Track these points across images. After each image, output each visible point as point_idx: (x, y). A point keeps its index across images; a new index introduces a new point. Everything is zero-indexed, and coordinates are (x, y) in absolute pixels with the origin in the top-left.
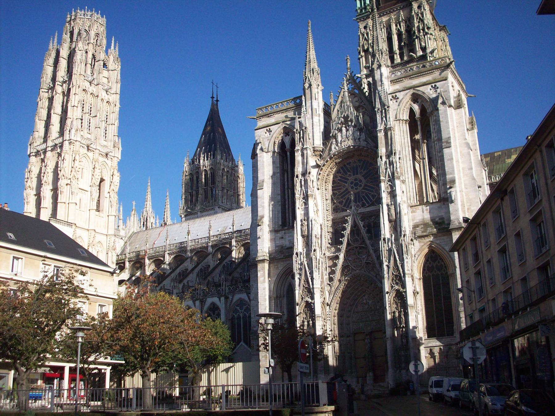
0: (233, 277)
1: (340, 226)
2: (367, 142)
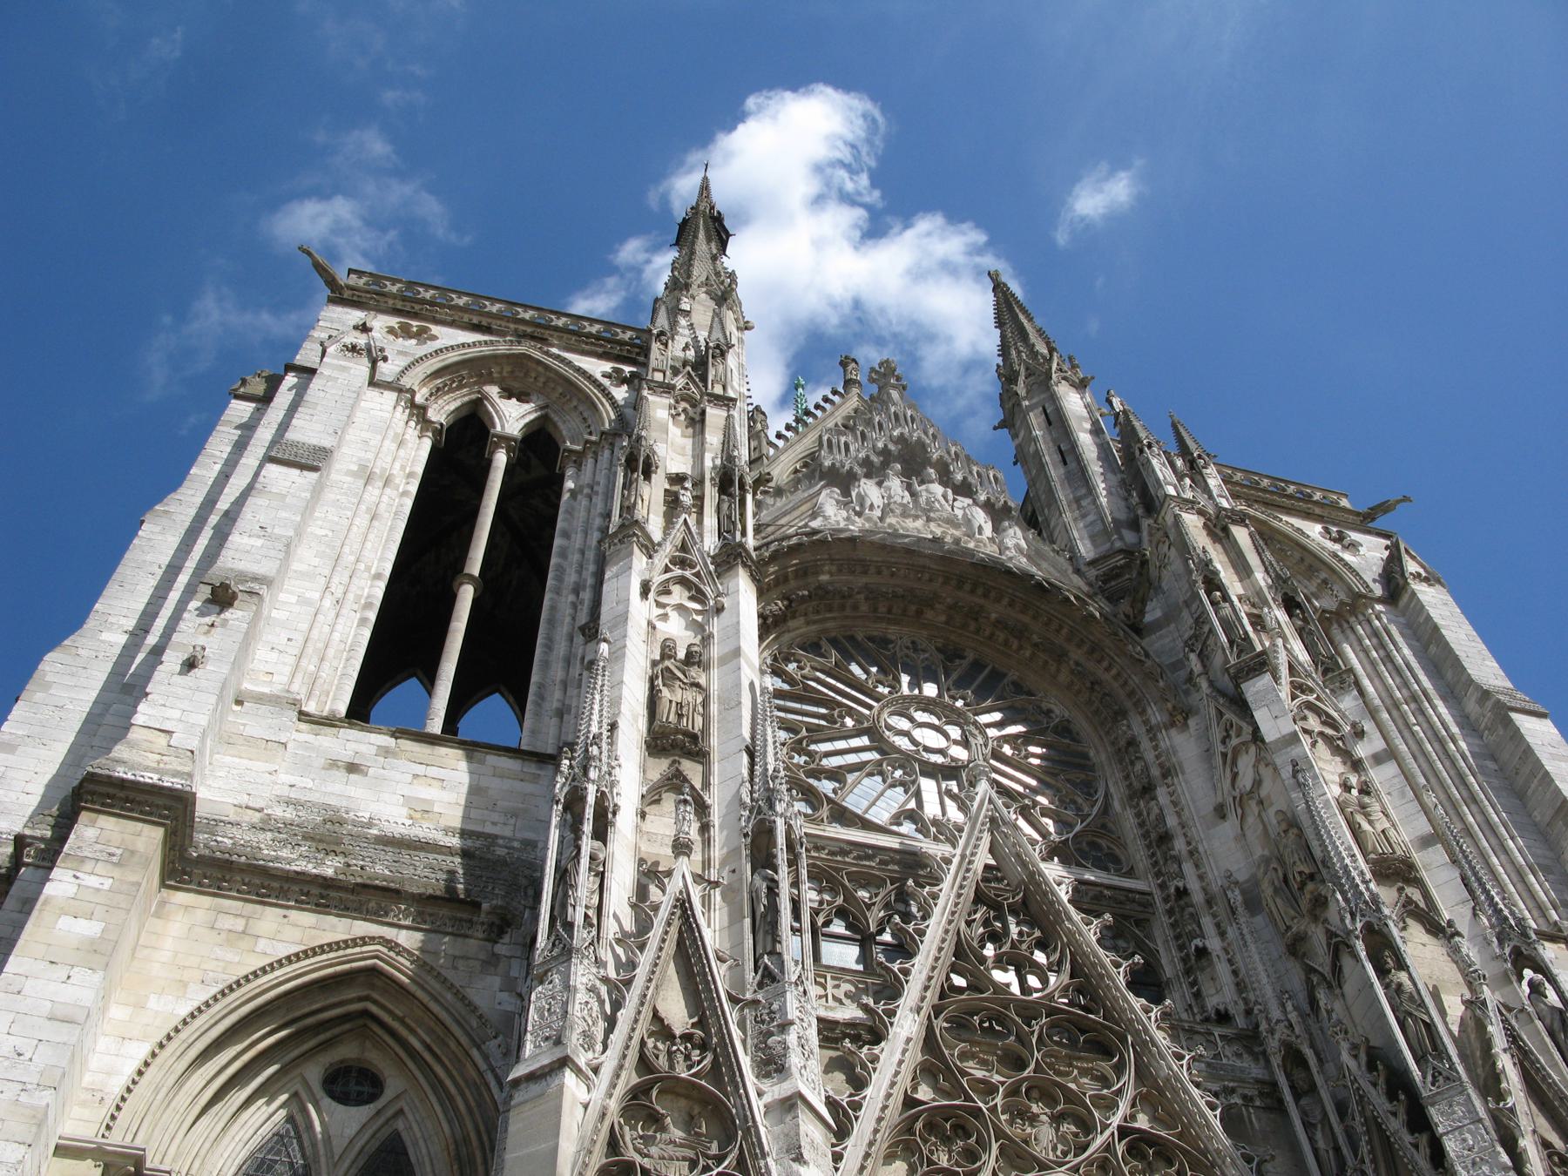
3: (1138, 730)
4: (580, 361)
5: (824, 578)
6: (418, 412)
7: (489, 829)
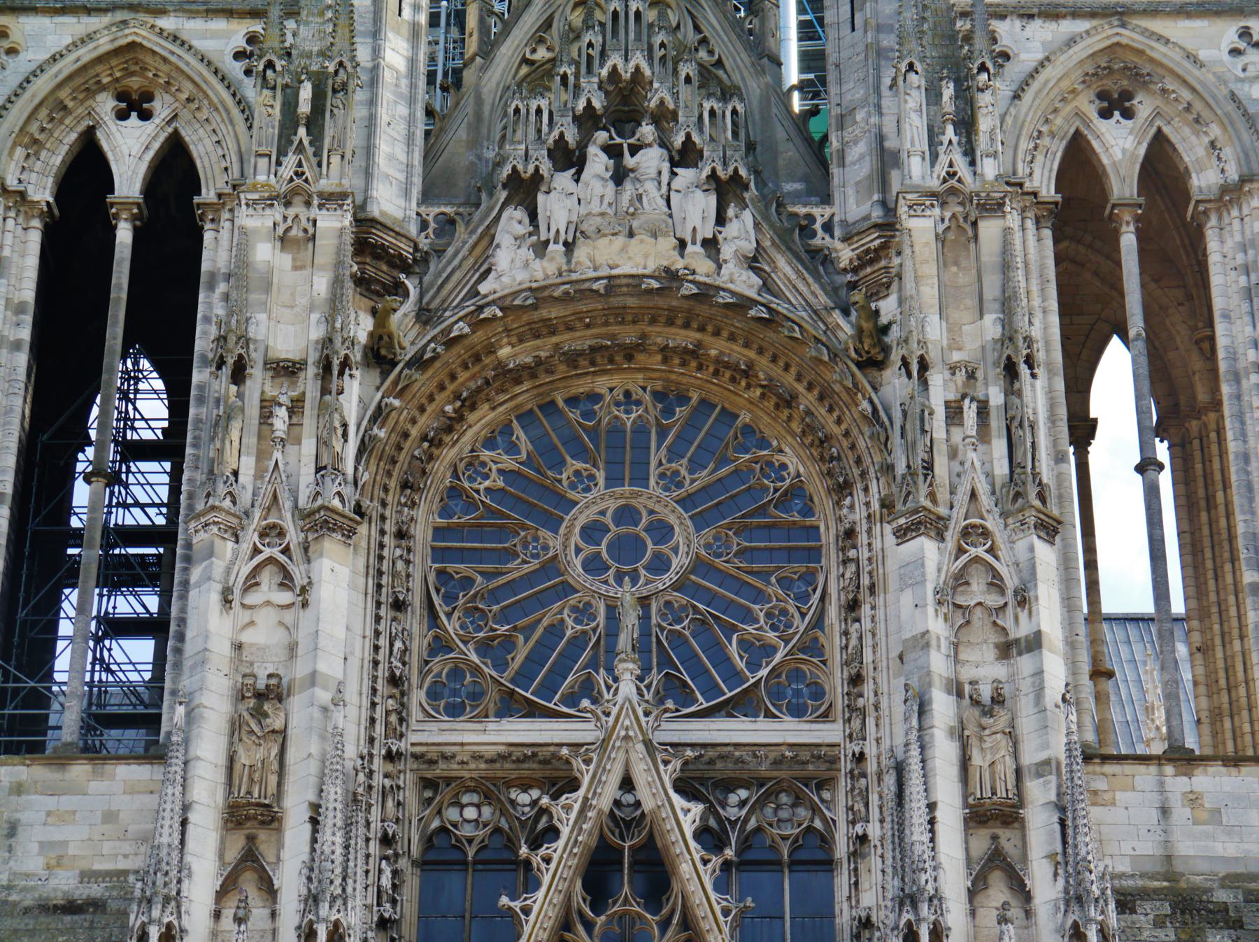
1: (470, 813)
2: (757, 271)
3: (859, 515)
4: (205, 35)
5: (504, 352)
7: (122, 865)
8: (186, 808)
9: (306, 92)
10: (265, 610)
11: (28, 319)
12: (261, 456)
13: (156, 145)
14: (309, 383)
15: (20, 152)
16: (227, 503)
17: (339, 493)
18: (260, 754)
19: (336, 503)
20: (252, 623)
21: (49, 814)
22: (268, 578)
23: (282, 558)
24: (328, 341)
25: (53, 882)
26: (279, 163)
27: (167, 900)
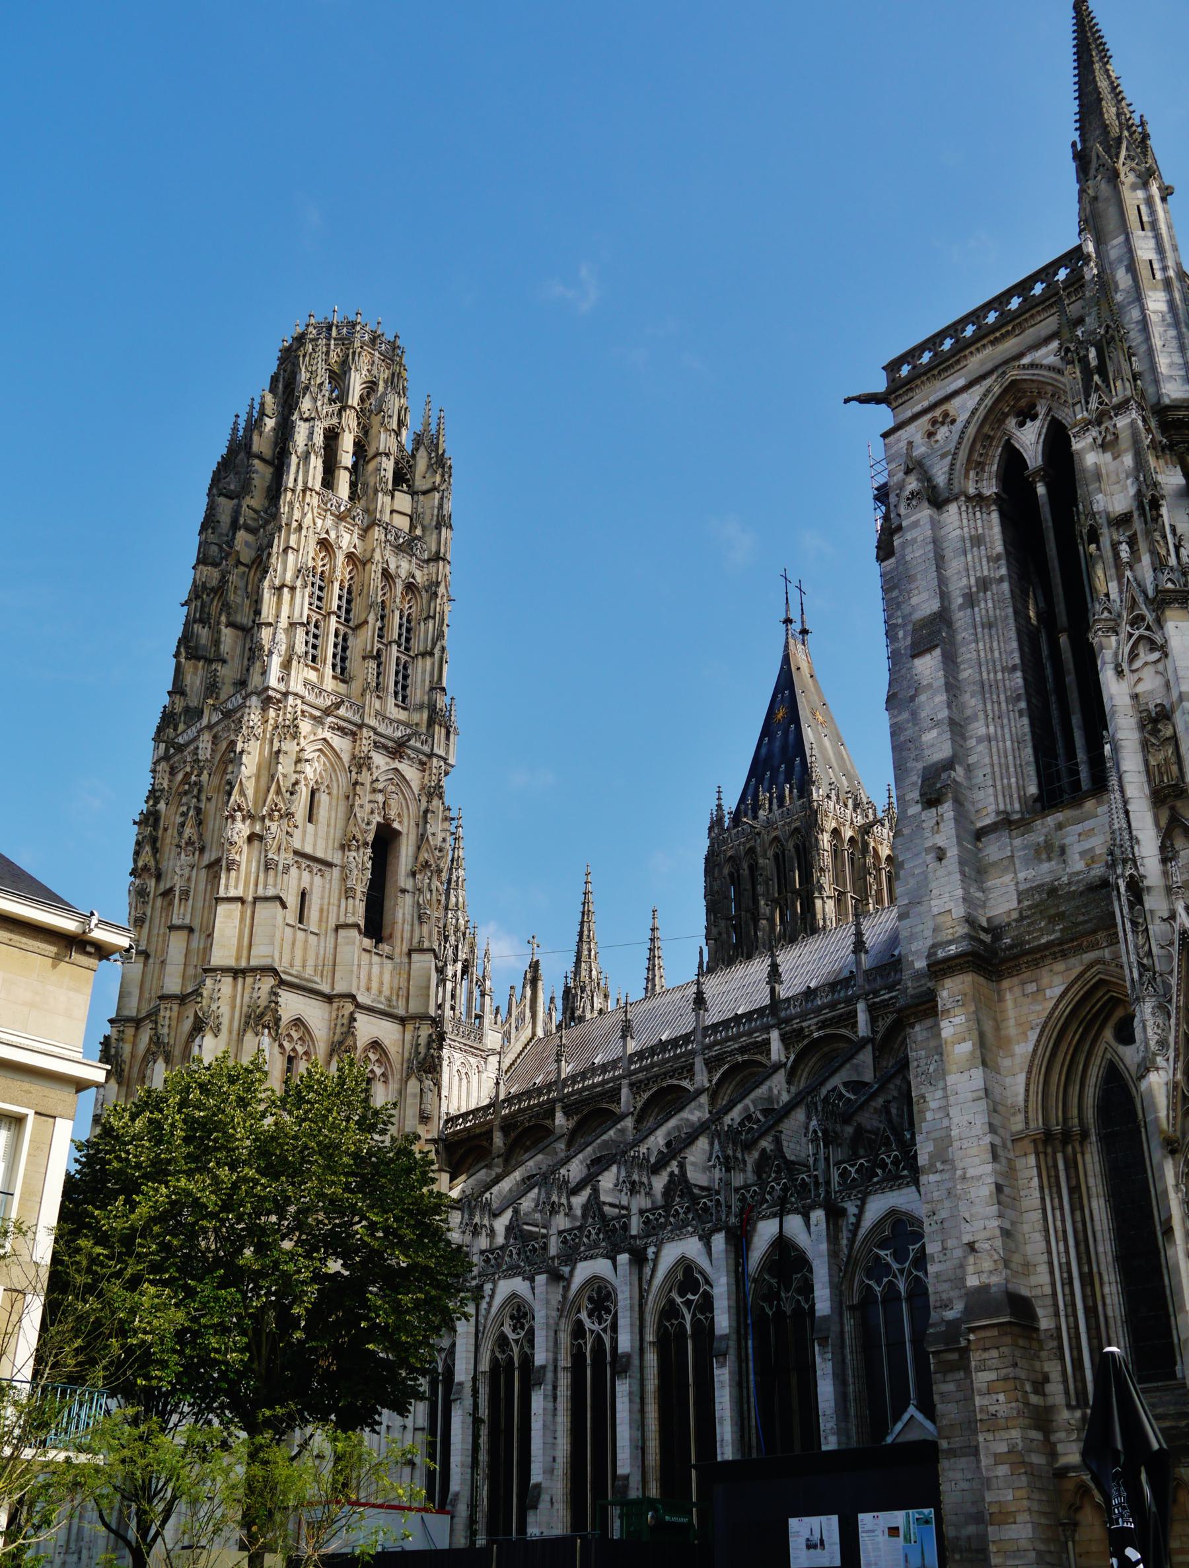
0: (859, 1129)
6: (978, 500)
8: (1125, 803)
9: (1092, 353)
10: (1146, 669)
11: (1003, 562)
12: (1120, 577)
13: (1044, 431)
14: (1138, 525)
15: (972, 474)
16: (1106, 614)
17: (1169, 579)
18: (1161, 756)
19: (1170, 585)
20: (1140, 680)
21: (1080, 835)
22: (1142, 649)
23: (1147, 633)
24: (1139, 494)
25: (1093, 873)
26: (1087, 403)
27: (1125, 861)
